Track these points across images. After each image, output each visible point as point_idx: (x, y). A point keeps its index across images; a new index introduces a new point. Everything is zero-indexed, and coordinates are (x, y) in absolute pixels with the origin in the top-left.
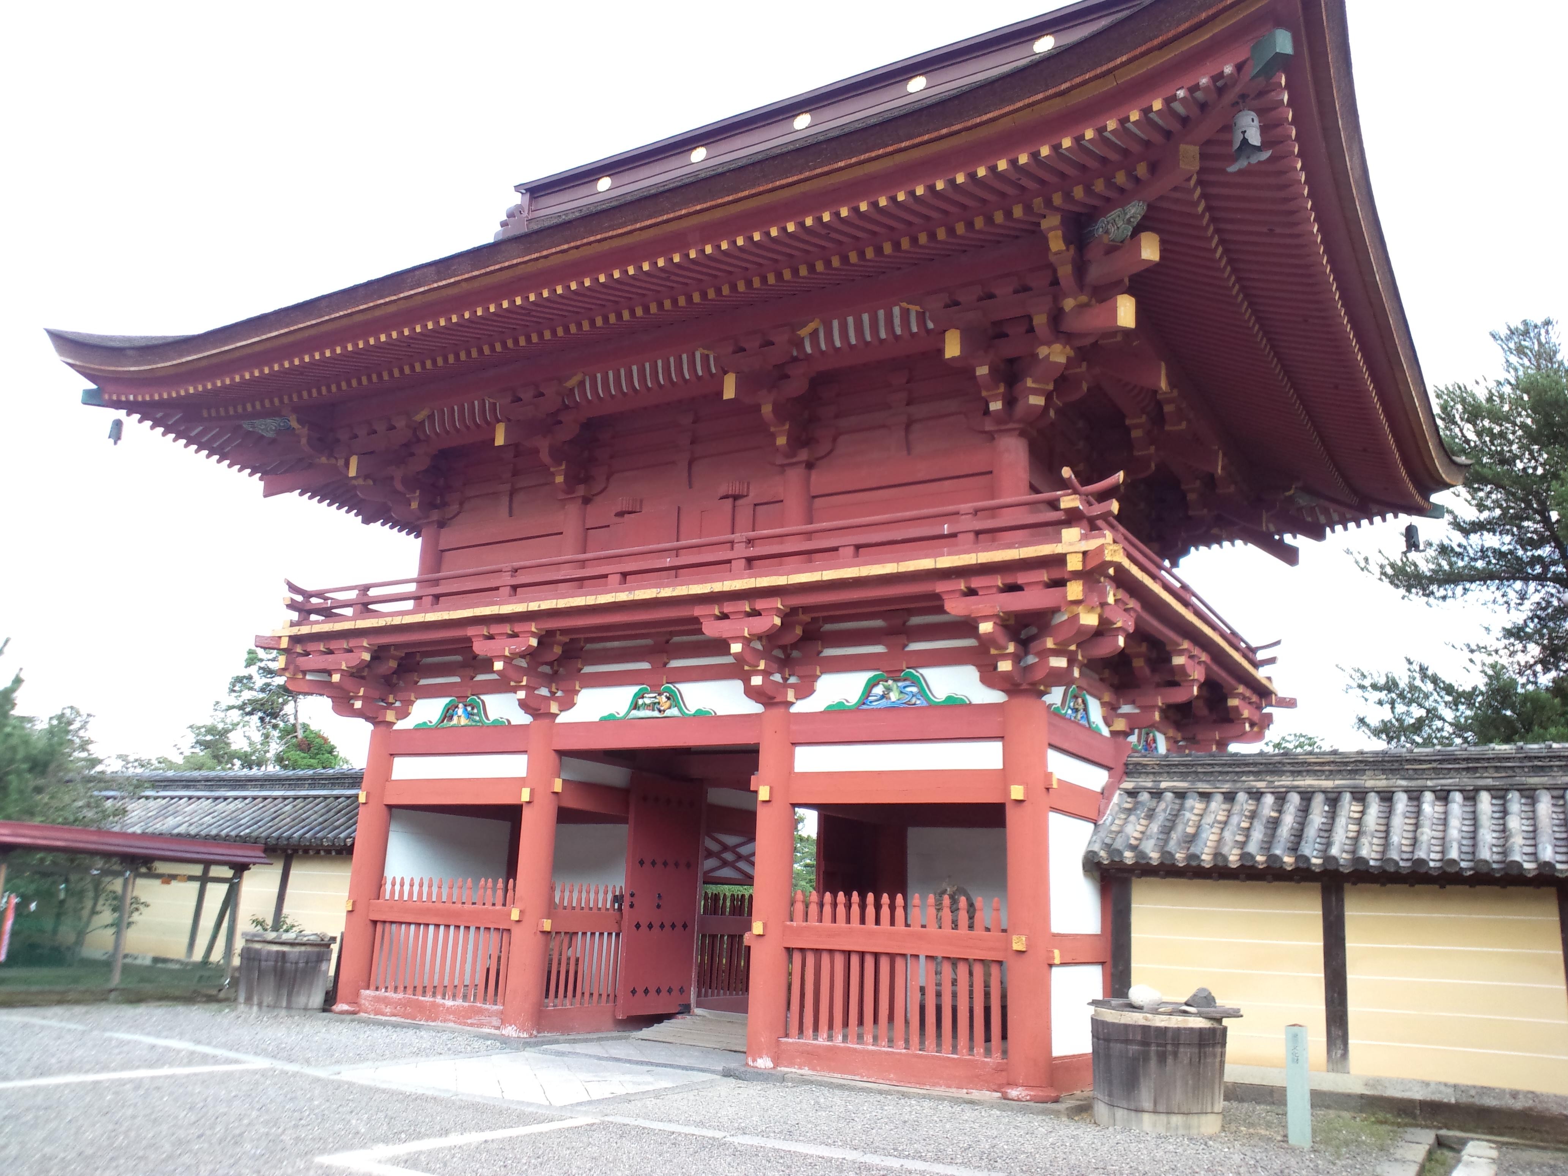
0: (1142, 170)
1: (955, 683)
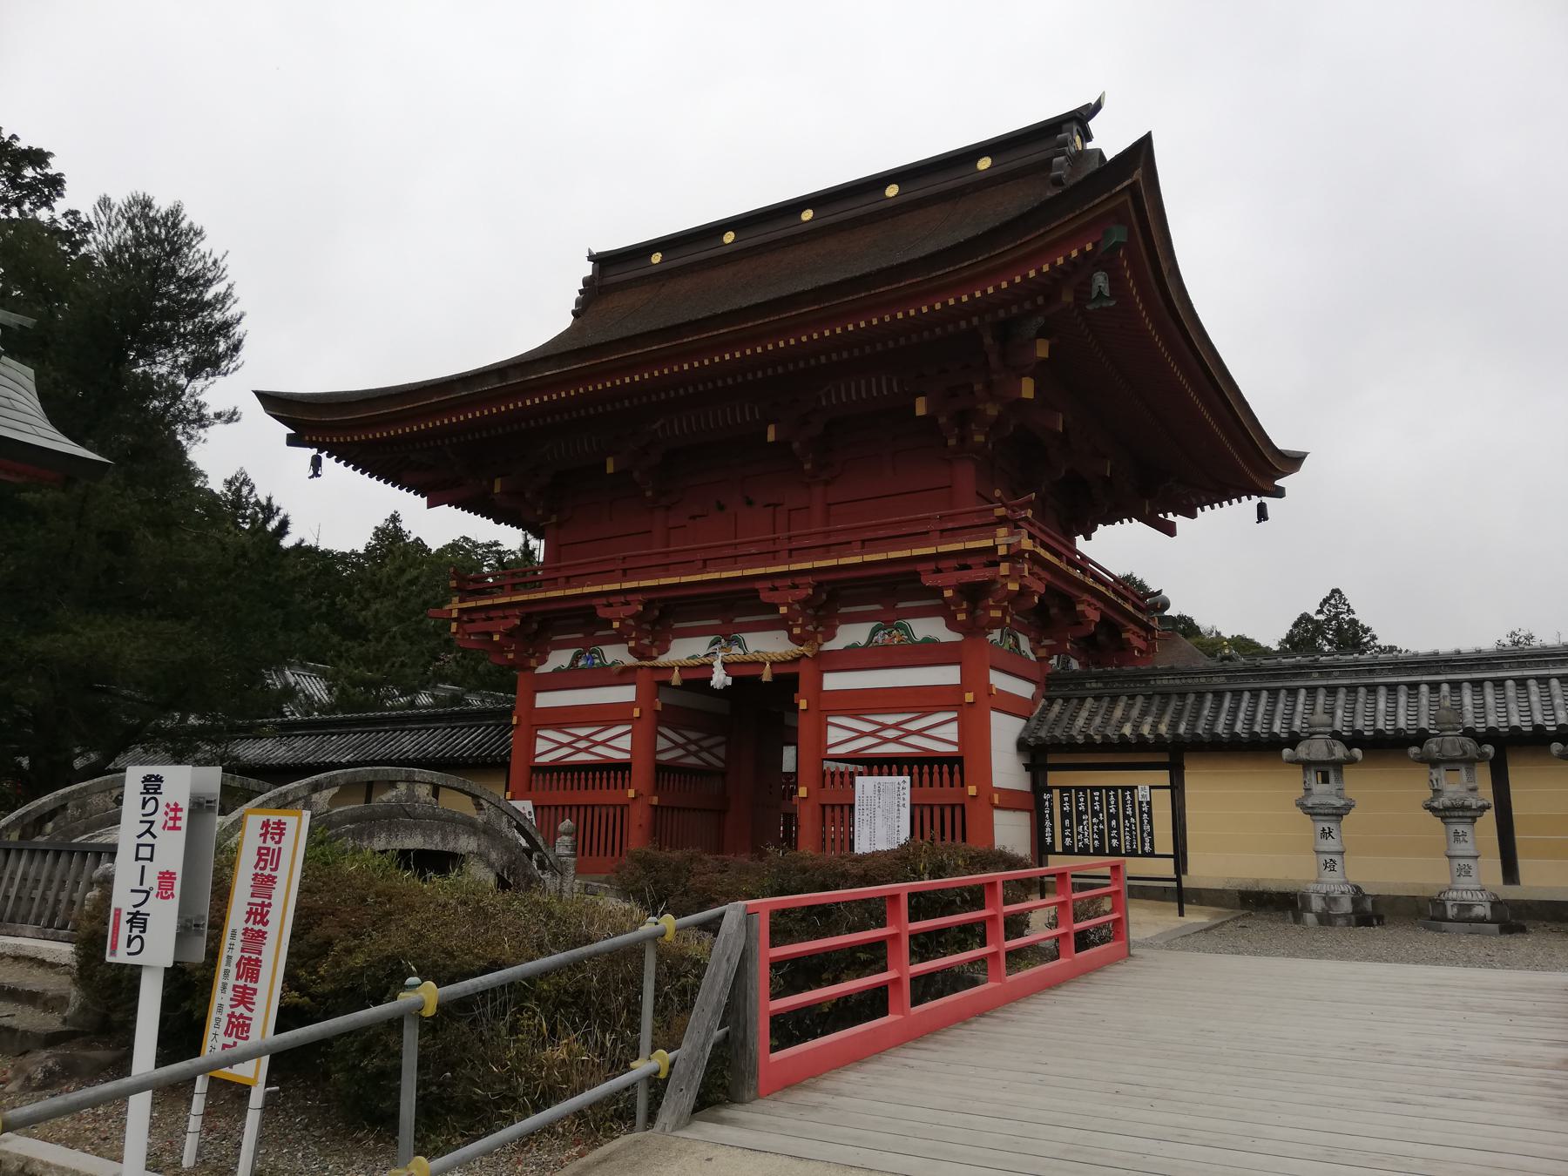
0: (1040, 300)
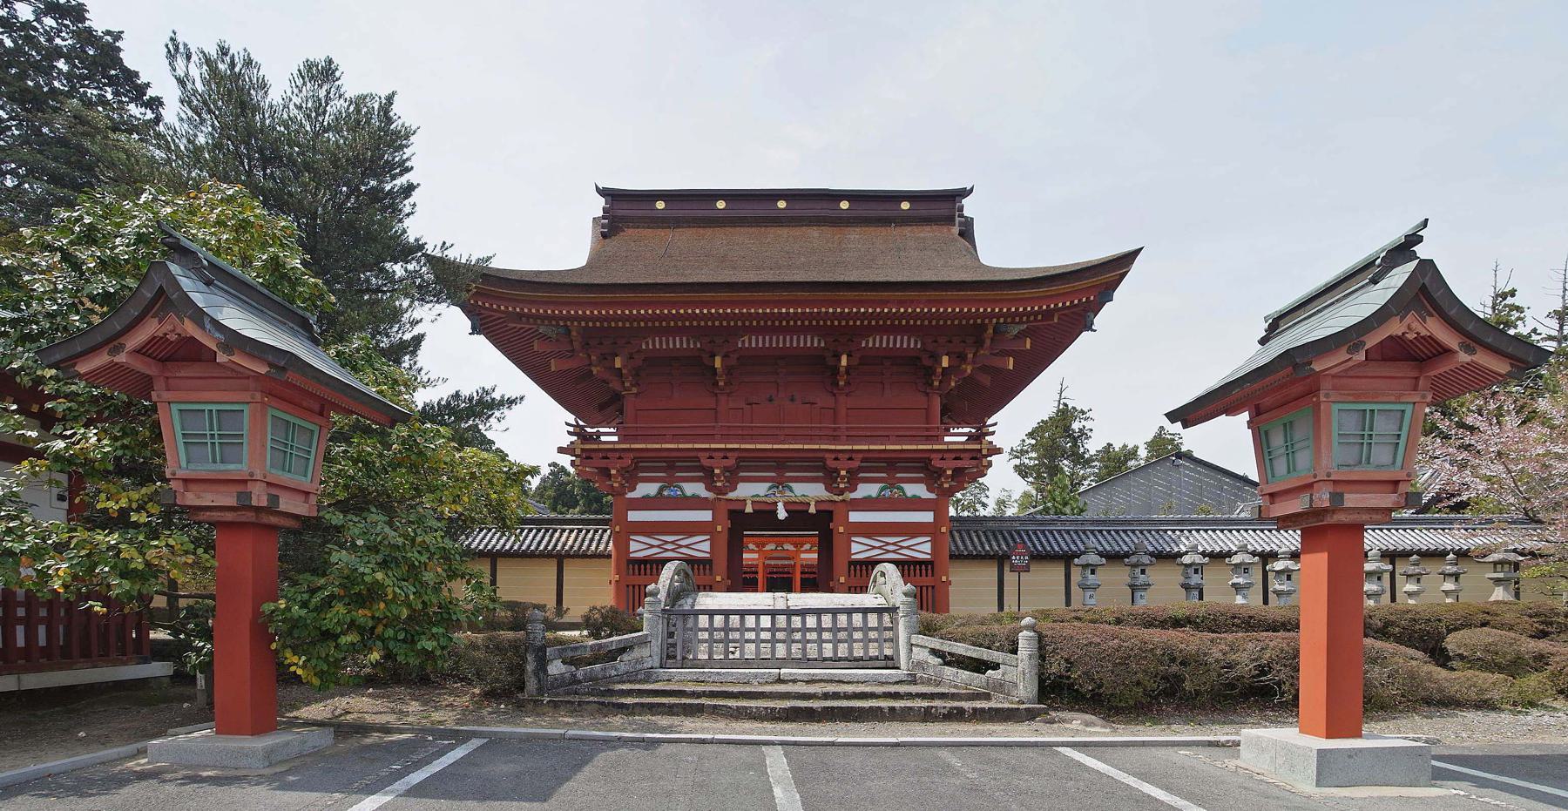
1: (918, 490)
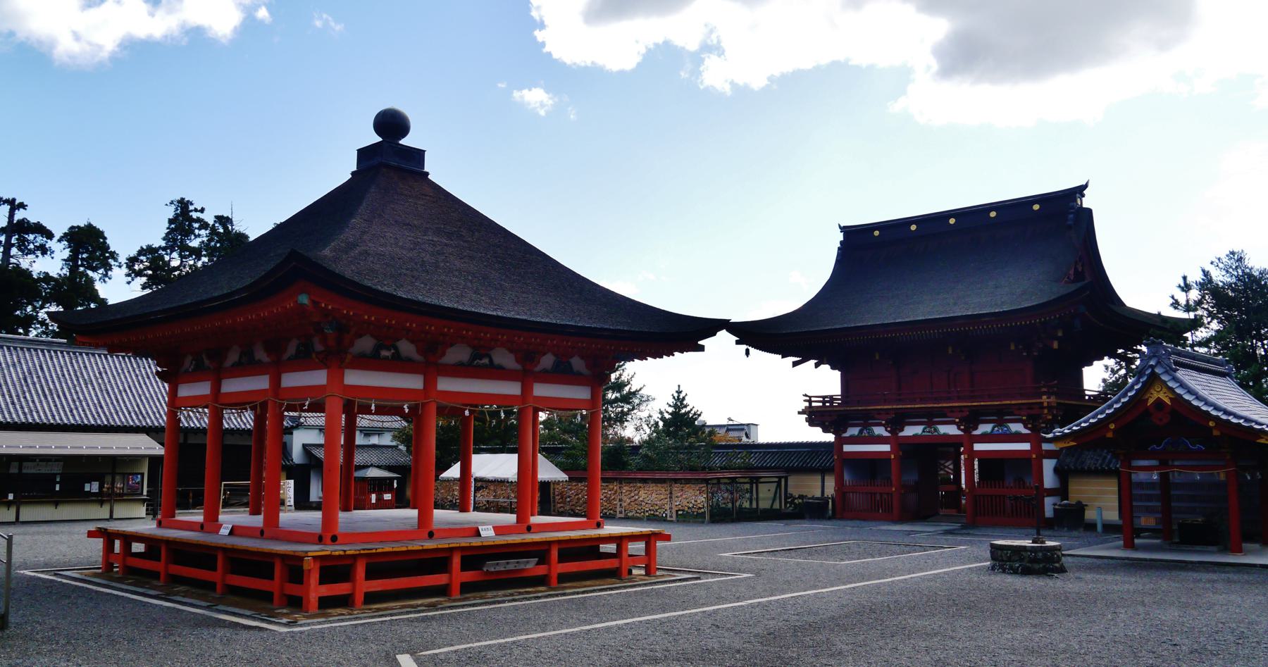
1: (1017, 427)
